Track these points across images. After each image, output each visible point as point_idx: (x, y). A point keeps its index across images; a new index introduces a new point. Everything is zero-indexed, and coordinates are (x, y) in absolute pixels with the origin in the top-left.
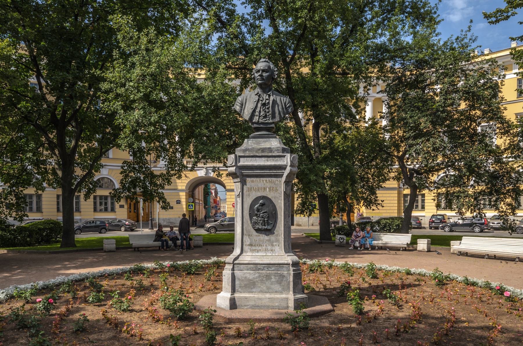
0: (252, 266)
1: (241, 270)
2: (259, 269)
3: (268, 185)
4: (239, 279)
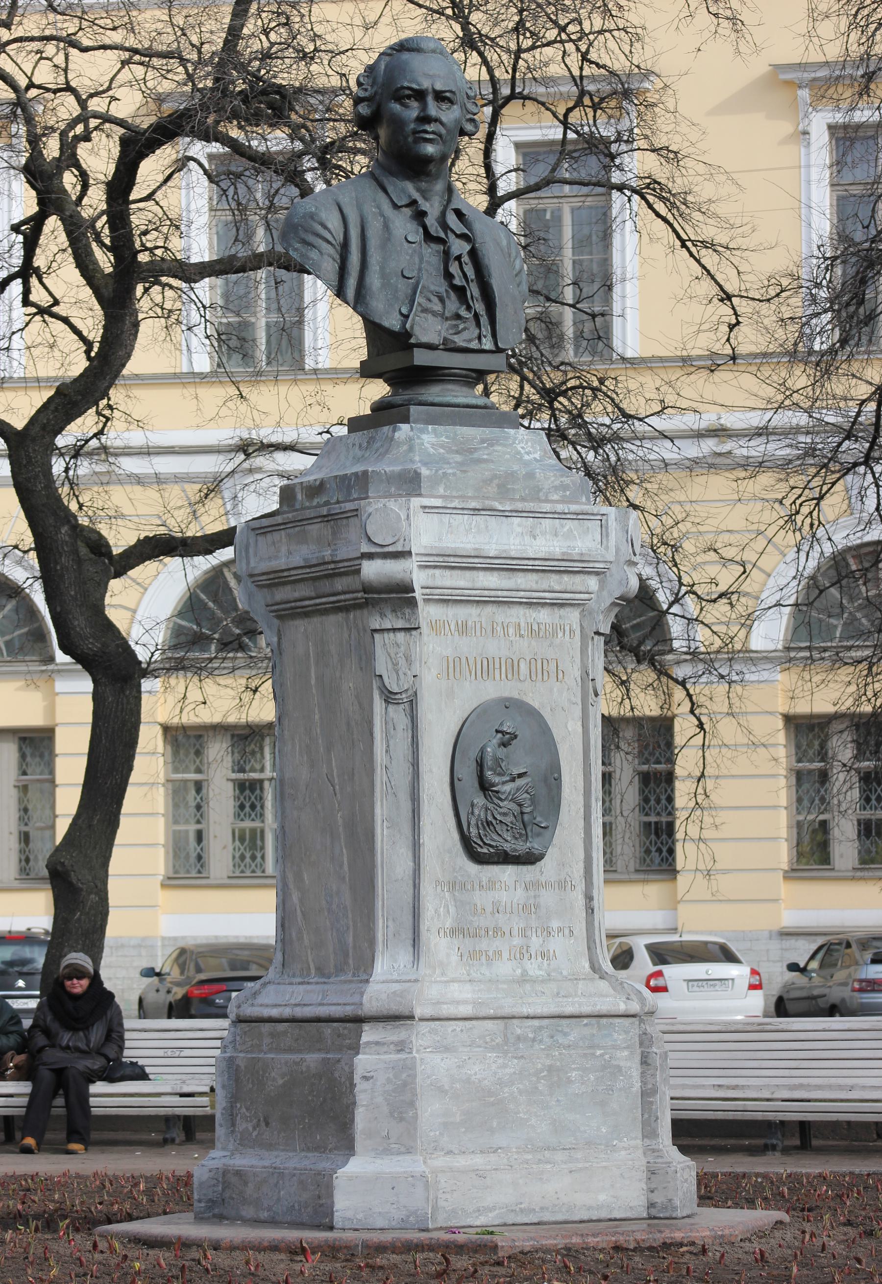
0: (489, 1024)
1: (447, 1049)
2: (519, 1038)
3: (524, 647)
4: (442, 1091)
